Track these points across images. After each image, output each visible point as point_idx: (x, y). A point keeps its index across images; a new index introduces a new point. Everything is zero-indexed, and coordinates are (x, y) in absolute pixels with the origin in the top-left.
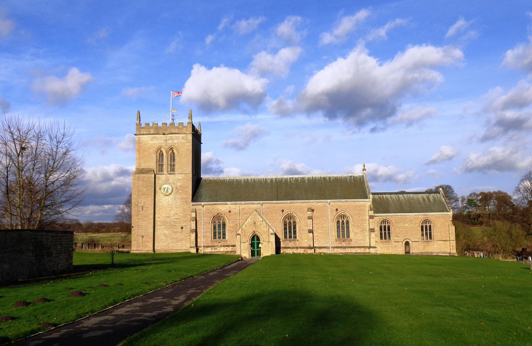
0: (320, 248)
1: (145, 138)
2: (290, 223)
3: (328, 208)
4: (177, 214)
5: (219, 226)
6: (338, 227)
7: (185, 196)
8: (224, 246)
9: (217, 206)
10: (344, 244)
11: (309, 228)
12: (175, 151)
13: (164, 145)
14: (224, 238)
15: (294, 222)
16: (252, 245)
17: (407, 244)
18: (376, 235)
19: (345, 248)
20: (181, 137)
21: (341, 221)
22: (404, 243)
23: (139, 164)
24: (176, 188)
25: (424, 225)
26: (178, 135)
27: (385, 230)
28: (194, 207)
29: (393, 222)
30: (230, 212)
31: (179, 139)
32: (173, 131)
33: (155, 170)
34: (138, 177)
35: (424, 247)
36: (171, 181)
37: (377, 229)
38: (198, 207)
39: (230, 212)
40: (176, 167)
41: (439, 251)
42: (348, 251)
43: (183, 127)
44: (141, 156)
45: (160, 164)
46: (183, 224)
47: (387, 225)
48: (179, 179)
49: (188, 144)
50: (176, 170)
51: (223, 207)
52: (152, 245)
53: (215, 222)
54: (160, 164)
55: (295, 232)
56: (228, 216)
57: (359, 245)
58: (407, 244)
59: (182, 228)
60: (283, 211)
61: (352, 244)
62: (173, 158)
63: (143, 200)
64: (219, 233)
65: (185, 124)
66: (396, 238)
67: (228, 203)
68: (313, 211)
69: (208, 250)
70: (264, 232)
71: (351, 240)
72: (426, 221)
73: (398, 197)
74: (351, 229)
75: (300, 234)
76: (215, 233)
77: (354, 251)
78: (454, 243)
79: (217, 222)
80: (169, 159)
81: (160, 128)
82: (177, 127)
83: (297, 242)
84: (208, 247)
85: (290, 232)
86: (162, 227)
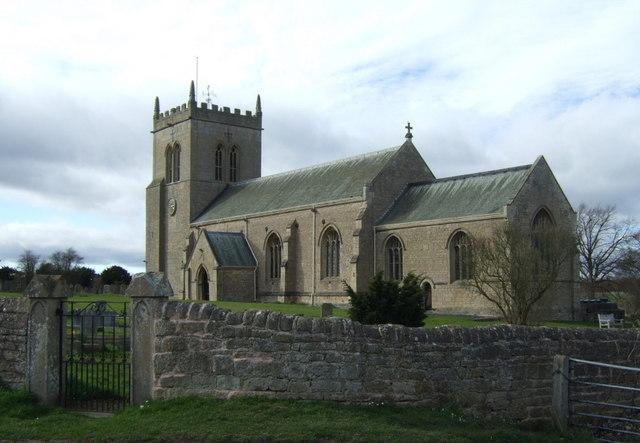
10: (330, 288)
19: (328, 295)
29: (405, 240)
72: (458, 235)
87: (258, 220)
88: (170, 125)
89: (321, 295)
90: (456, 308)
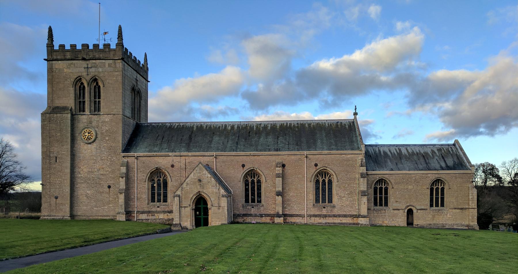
0: (292, 216)
1: (59, 65)
2: (253, 182)
3: (302, 164)
4: (103, 168)
5: (159, 185)
6: (317, 188)
7: (113, 145)
8: (164, 212)
9: (156, 159)
10: (324, 212)
11: (277, 189)
12: (100, 84)
13: (84, 74)
14: (165, 201)
15: (259, 182)
16: (196, 209)
17: (410, 212)
18: (368, 200)
19: (325, 216)
20: (107, 66)
21: (321, 180)
22: (406, 211)
23: (52, 100)
24: (102, 134)
25: (435, 188)
26: (104, 61)
27: (381, 193)
28: (125, 160)
29: (393, 181)
30: (173, 166)
31: (105, 66)
32: (97, 56)
33: (73, 108)
34: (50, 118)
35: (434, 216)
36: (94, 124)
37: (372, 191)
38: (130, 160)
39: (173, 166)
41: (454, 222)
42: (330, 220)
43: (110, 50)
44: (54, 89)
45: (80, 102)
46: (111, 183)
47: (384, 187)
48: (104, 122)
49: (117, 73)
50: (102, 110)
51: (163, 160)
52: (68, 209)
53: (153, 180)
54: (80, 102)
55: (259, 195)
56: (170, 172)
57: (345, 213)
58: (410, 212)
59: (109, 187)
60: (243, 166)
61: (336, 212)
62: (97, 93)
63: (56, 149)
64: (159, 195)
65: (113, 46)
66: (395, 204)
67: (170, 154)
68: (284, 166)
69: (144, 216)
70: (213, 193)
71: (334, 207)
72: (438, 181)
73: (400, 150)
74: (334, 192)
75: (232, 187)
76: (153, 194)
77: (337, 220)
78: (474, 213)
79: (156, 180)
80: (93, 94)
81: (80, 51)
82: (102, 51)
83: (262, 208)
84: (143, 213)
85: (253, 194)
86: (83, 185)
87: (232, 158)
88: (84, 59)
89: (315, 216)
90: (434, 224)
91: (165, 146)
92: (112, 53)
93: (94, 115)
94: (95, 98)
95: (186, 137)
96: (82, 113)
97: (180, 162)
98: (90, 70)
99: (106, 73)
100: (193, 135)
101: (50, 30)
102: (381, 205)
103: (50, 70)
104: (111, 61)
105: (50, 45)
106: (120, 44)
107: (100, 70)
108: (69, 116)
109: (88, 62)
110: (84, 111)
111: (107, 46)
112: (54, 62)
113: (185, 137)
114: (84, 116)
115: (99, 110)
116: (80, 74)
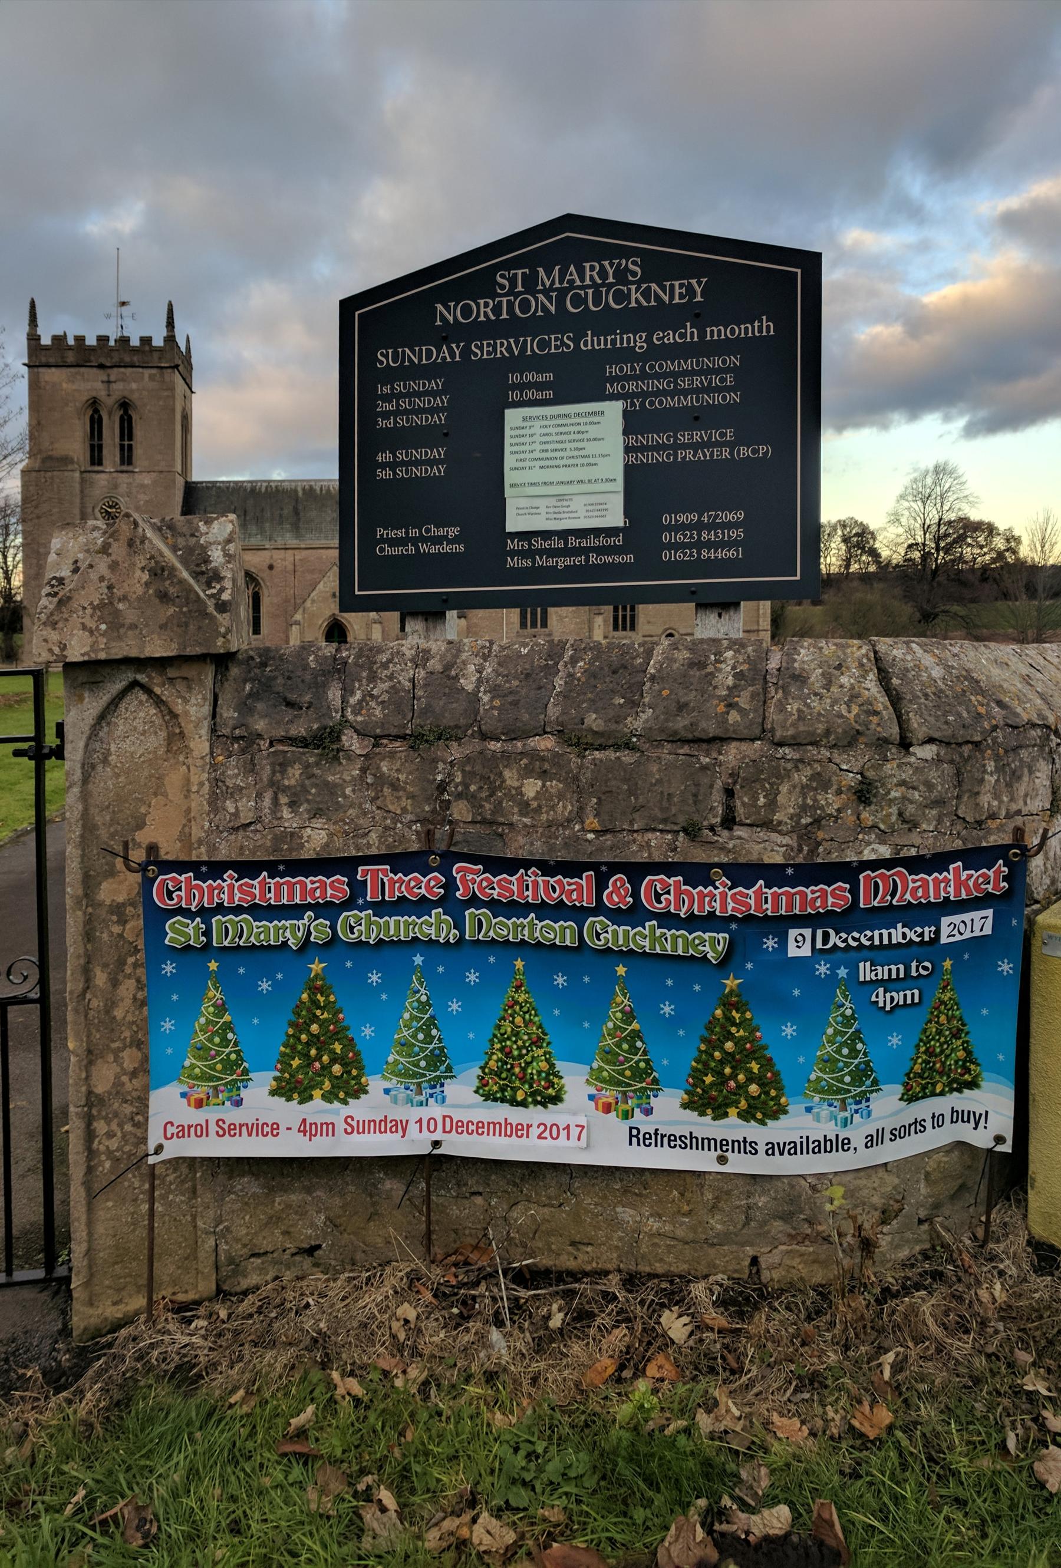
1: (52, 375)
13: (102, 394)
18: (605, 621)
20: (146, 376)
30: (271, 567)
31: (142, 378)
36: (123, 488)
39: (271, 567)
40: (138, 452)
48: (142, 486)
65: (158, 342)
81: (92, 349)
82: (135, 350)
88: (101, 366)
91: (253, 529)
92: (156, 355)
93: (122, 472)
94: (122, 438)
95: (287, 511)
96: (97, 468)
97: (284, 559)
98: (114, 386)
99: (145, 393)
100: (300, 507)
101: (33, 305)
102: (624, 629)
103: (34, 386)
104: (154, 371)
105: (33, 338)
106: (170, 339)
107: (134, 386)
108: (77, 475)
109: (109, 371)
110: (100, 463)
111: (146, 341)
112: (41, 370)
113: (285, 512)
114: (103, 476)
115: (130, 463)
116: (94, 394)
